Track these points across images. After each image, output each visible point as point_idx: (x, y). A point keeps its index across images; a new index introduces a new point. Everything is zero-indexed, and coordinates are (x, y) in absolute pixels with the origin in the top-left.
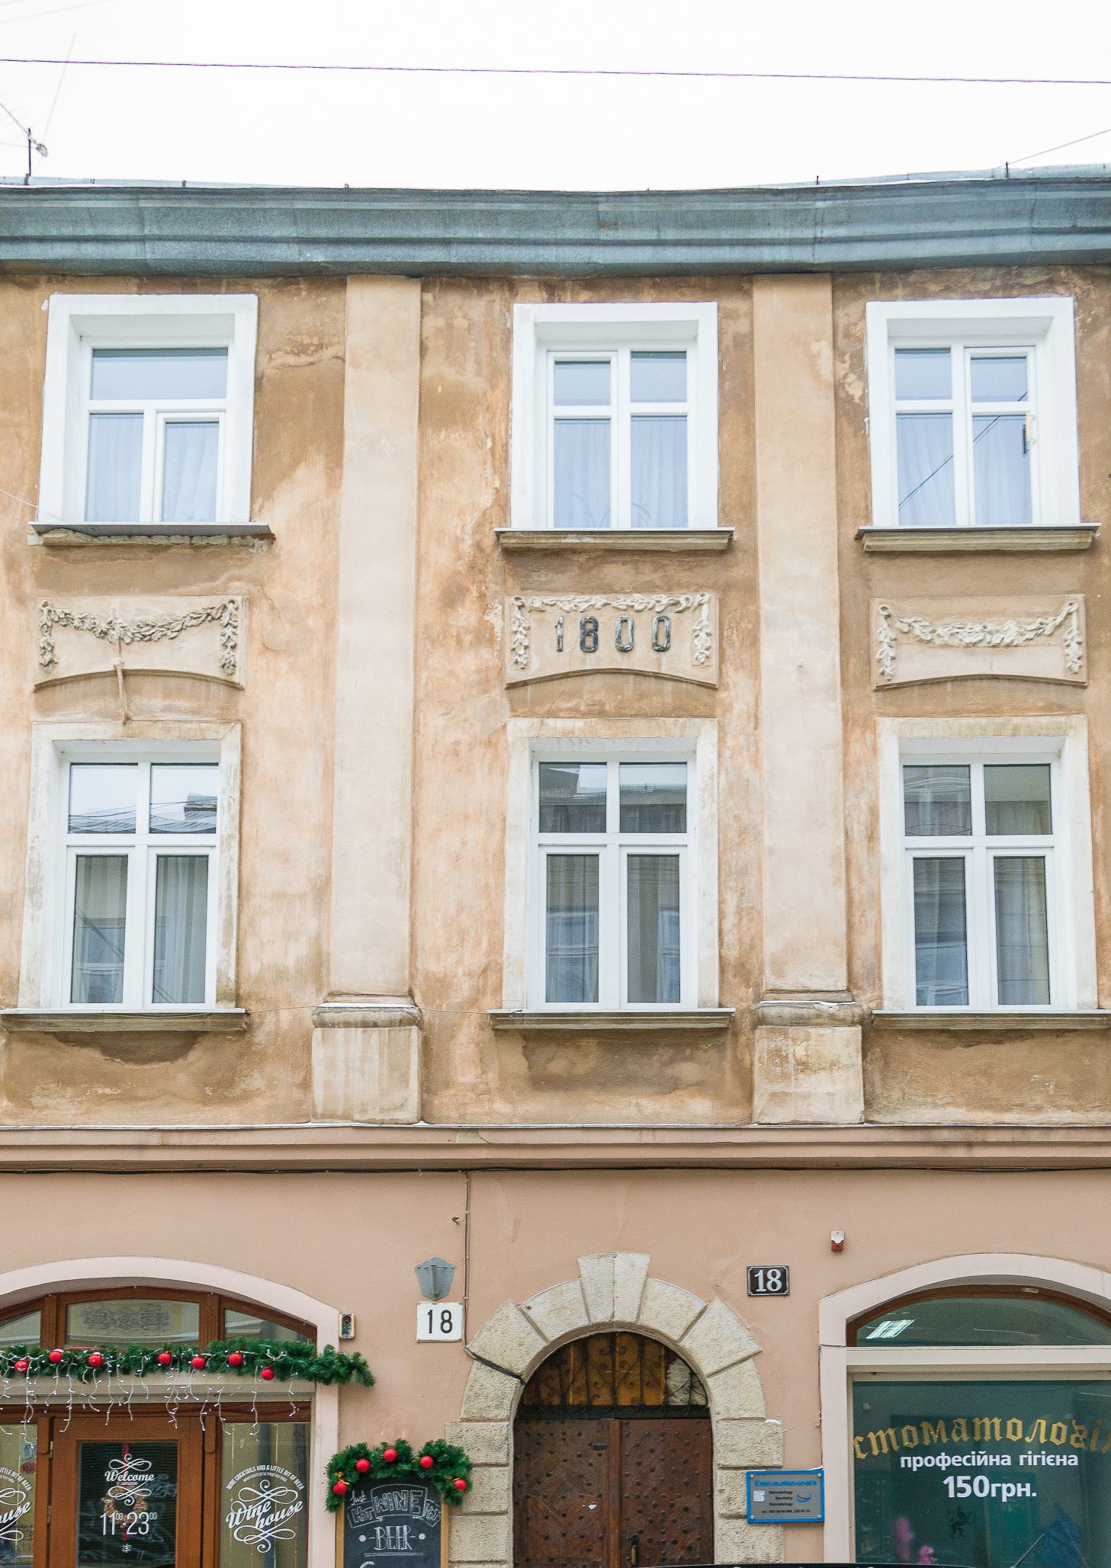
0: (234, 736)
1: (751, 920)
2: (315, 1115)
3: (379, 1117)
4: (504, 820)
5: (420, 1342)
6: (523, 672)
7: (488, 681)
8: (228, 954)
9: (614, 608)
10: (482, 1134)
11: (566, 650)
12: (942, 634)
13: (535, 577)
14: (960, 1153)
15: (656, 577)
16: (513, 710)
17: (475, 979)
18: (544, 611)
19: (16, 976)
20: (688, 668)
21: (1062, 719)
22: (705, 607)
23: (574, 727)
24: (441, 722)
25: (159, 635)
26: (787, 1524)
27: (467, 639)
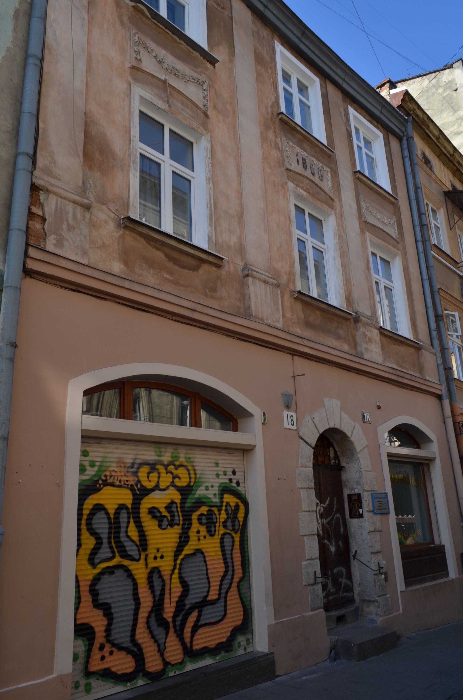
0: (208, 136)
2: (252, 316)
5: (285, 428)
8: (212, 229)
10: (304, 341)
14: (401, 380)
19: (126, 200)
21: (396, 250)
25: (181, 77)
26: (382, 514)
27: (273, 144)
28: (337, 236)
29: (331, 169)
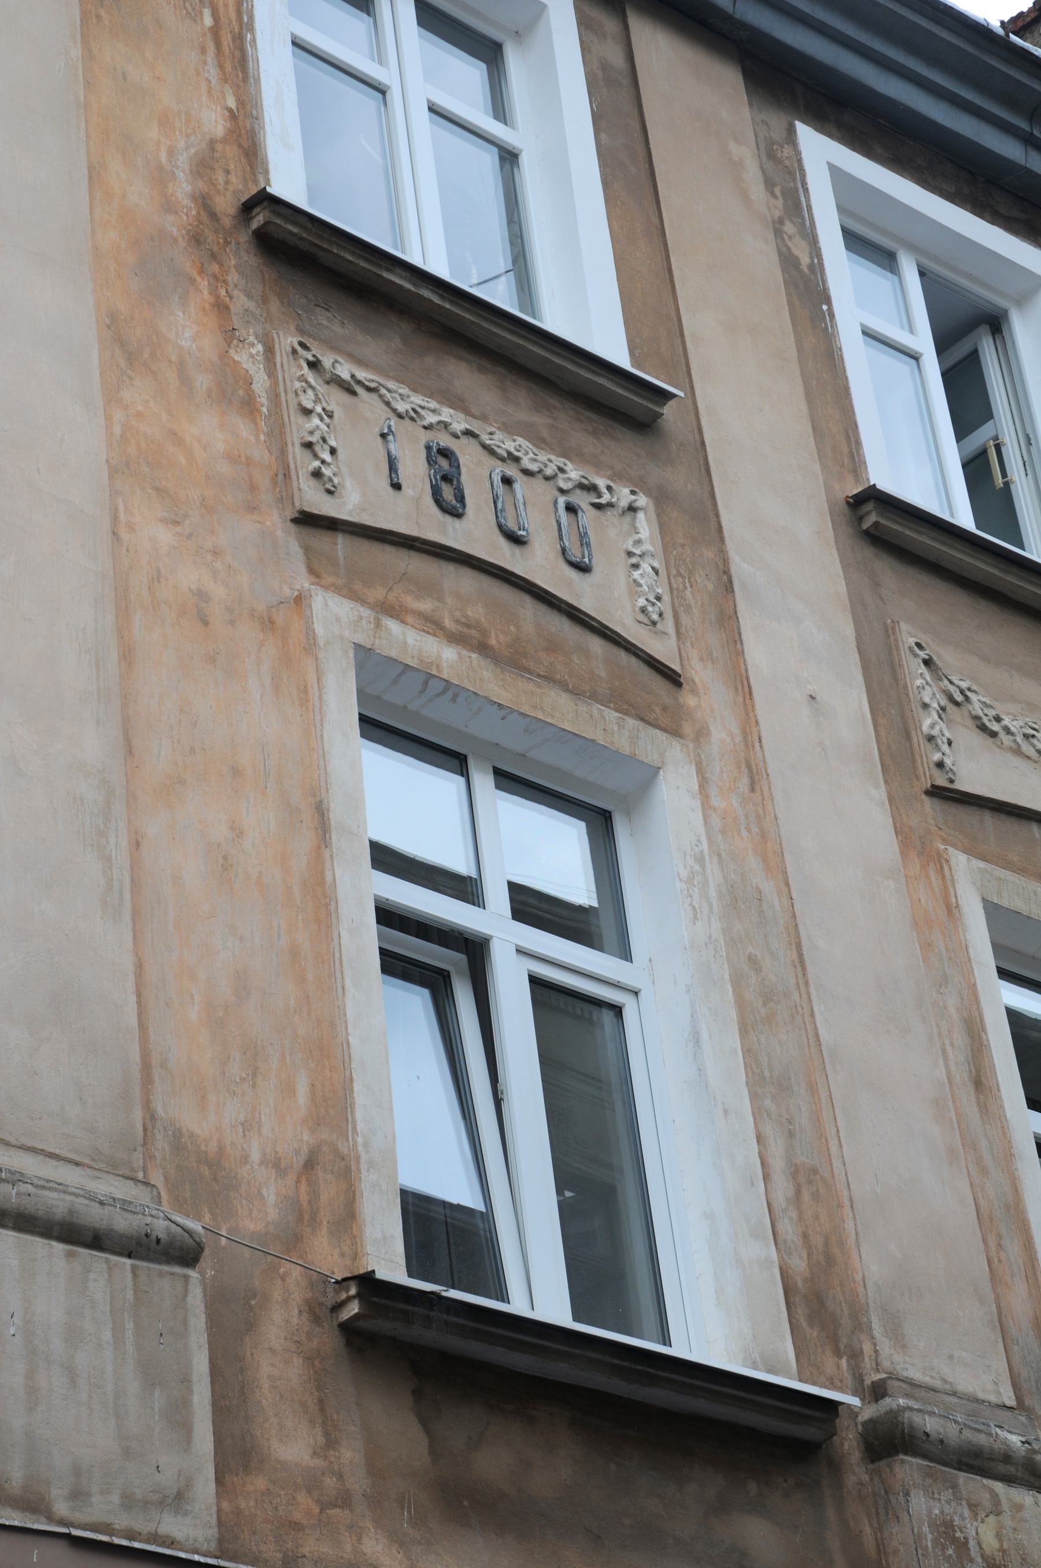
1: (816, 1196)
3: (121, 1521)
4: (321, 811)
6: (327, 497)
7: (253, 488)
9: (485, 447)
11: (408, 490)
12: (1013, 729)
13: (322, 317)
15: (540, 421)
16: (312, 571)
17: (291, 1178)
18: (354, 393)
20: (629, 621)
22: (641, 515)
23: (439, 657)
24: (165, 536)
27: (202, 381)
28: (713, 893)
29: (662, 498)
